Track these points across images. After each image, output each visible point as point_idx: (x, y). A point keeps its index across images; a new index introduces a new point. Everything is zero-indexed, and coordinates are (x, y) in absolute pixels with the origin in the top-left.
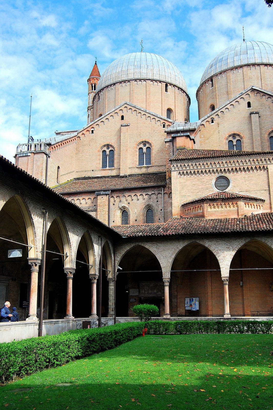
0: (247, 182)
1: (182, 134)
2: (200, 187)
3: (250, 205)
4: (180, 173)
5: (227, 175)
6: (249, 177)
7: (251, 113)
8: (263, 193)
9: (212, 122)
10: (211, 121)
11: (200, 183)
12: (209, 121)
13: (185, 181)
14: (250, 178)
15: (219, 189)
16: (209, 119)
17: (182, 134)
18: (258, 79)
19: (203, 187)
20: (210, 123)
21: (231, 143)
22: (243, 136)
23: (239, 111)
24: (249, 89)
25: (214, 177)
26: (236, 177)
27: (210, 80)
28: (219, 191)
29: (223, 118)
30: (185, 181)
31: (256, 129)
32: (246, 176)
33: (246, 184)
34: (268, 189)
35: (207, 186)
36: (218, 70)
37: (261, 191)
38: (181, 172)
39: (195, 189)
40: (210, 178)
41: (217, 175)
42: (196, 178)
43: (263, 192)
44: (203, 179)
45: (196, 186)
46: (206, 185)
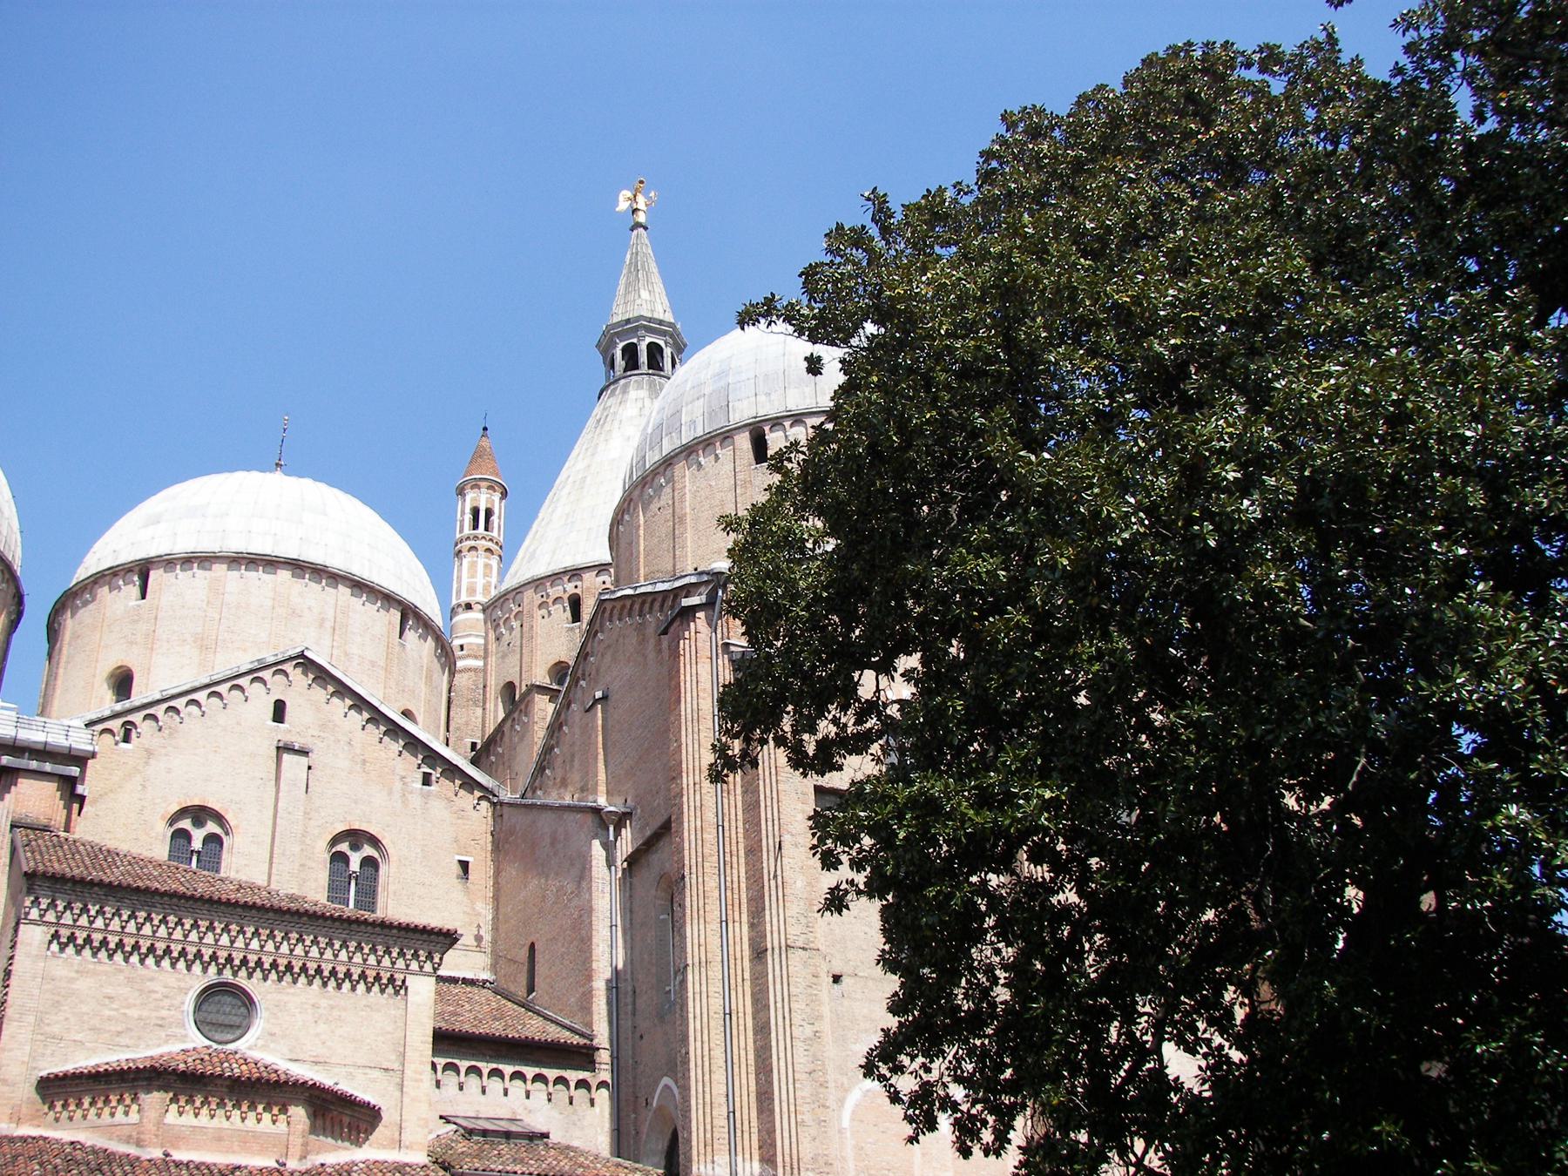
0: (322, 1027)
1: (48, 767)
2: (134, 1013)
3: (328, 1123)
4: (56, 936)
5: (253, 985)
6: (332, 1007)
7: (283, 749)
8: (374, 1081)
9: (127, 739)
10: (122, 734)
11: (137, 994)
12: (115, 731)
13: (73, 975)
14: (336, 1013)
15: (210, 1035)
16: (116, 725)
17: (48, 767)
18: (321, 626)
19: (145, 1013)
20: (117, 738)
21: (182, 841)
22: (237, 827)
23: (239, 724)
24: (292, 653)
25: (199, 979)
26: (286, 998)
27: (137, 569)
28: (208, 1043)
29: (170, 734)
30: (73, 975)
31: (290, 809)
32: (324, 1003)
33: (317, 1035)
34: (396, 1066)
35: (164, 1013)
36: (182, 547)
37: (368, 1070)
38: (64, 933)
39: (110, 1019)
40: (182, 985)
41: (212, 974)
42: (121, 971)
43: (377, 1074)
44: (152, 979)
45: (114, 1006)
46: (157, 1009)
